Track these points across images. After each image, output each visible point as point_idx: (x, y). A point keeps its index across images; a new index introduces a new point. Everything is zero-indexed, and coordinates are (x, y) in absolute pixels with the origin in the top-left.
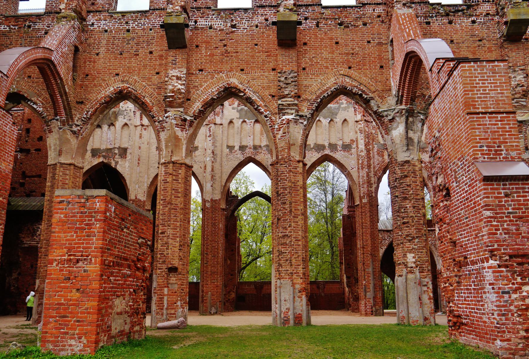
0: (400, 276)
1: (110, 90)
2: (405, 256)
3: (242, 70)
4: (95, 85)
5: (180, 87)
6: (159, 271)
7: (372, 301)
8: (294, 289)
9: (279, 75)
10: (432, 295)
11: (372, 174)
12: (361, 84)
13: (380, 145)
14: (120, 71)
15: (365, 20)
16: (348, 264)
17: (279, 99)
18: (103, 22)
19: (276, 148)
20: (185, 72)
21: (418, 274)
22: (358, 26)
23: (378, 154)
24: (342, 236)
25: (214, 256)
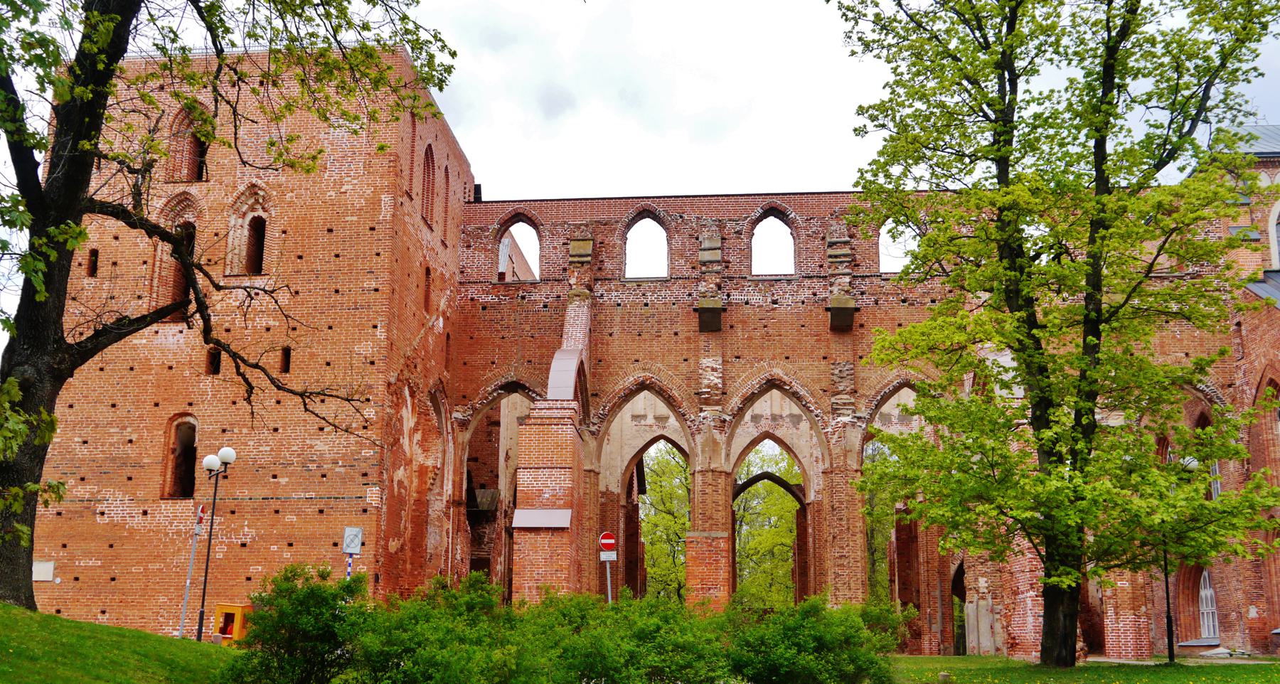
0: (971, 602)
1: (630, 381)
2: (976, 580)
3: (787, 358)
4: (610, 373)
5: (717, 381)
7: (939, 635)
9: (833, 367)
12: (928, 377)
14: (640, 356)
15: (934, 296)
16: (904, 584)
17: (833, 396)
18: (614, 294)
19: (830, 455)
20: (720, 362)
21: (990, 600)
22: (925, 304)
24: (893, 539)
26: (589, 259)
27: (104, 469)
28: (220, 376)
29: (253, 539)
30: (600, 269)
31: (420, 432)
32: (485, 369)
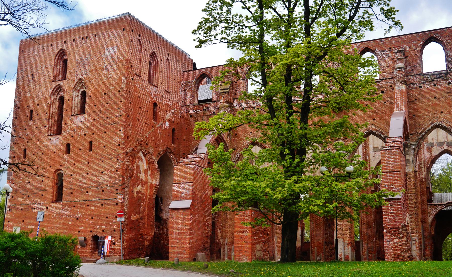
4: (240, 139)
6: (278, 235)
8: (344, 243)
10: (418, 246)
11: (422, 166)
12: (380, 129)
13: (429, 144)
23: (427, 150)
25: (318, 224)
26: (228, 90)
27: (35, 192)
28: (70, 154)
29: (80, 216)
30: (236, 94)
31: (150, 171)
32: (191, 142)
